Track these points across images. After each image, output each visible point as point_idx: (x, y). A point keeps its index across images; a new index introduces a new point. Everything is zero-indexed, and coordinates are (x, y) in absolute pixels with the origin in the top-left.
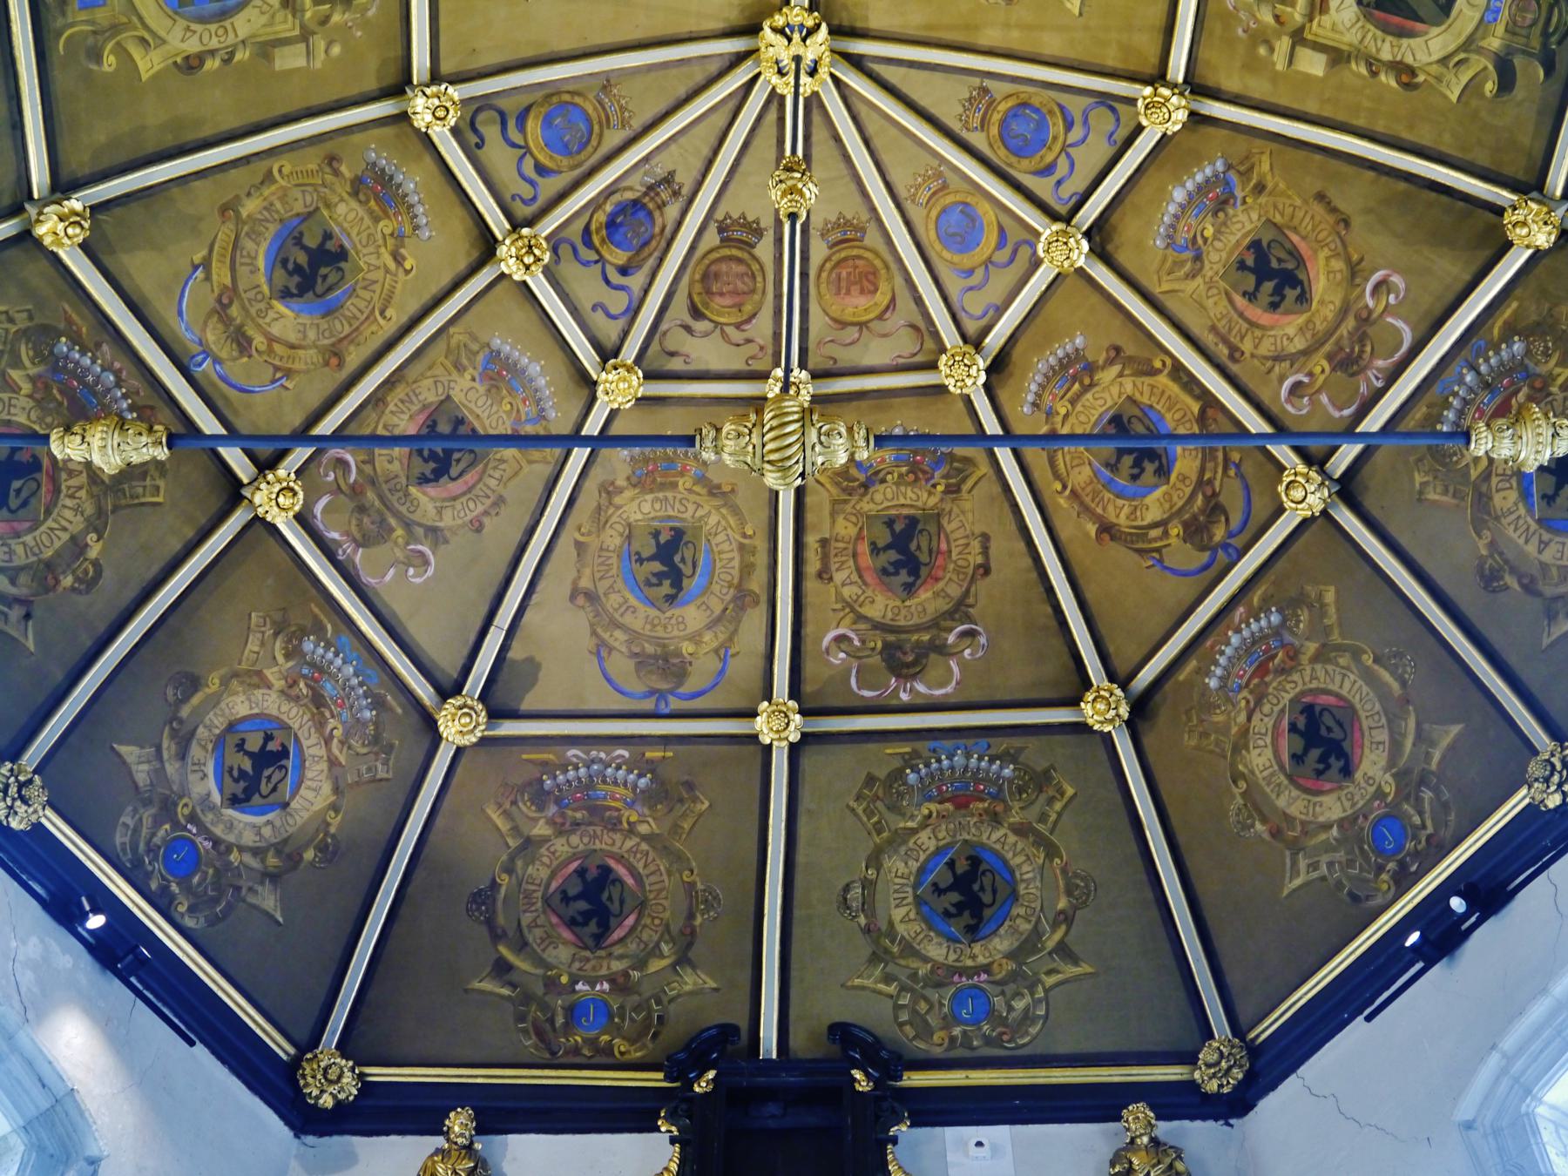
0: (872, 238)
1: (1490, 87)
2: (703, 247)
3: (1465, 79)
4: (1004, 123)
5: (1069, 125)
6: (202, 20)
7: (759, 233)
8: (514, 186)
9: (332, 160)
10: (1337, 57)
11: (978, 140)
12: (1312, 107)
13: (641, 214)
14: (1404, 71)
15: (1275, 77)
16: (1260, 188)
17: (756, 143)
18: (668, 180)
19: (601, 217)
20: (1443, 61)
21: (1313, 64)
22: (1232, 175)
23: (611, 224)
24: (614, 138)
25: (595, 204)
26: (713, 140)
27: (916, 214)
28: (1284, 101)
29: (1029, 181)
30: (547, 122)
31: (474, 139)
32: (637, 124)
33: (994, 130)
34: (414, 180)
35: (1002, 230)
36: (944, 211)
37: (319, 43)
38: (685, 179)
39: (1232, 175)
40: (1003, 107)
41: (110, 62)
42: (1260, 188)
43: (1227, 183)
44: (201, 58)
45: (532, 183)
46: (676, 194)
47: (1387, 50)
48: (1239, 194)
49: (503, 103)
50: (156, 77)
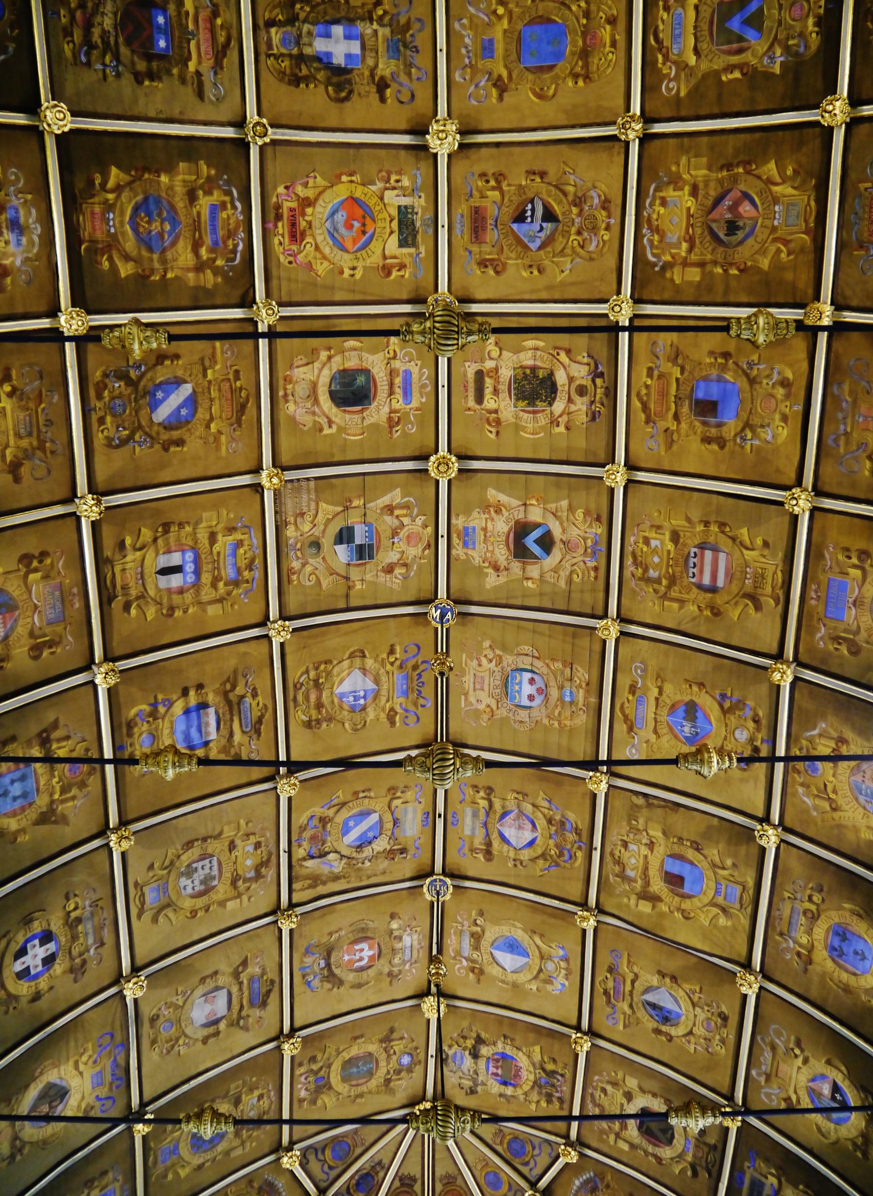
0: (459, 1181)
1: (689, 1173)
2: (394, 1187)
3: (680, 1167)
4: (509, 1143)
5: (534, 1148)
6: (205, 1151)
7: (415, 1181)
8: (320, 1175)
9: (250, 1182)
10: (633, 1146)
11: (499, 1148)
12: (625, 1160)
13: (370, 1179)
14: (659, 1160)
15: (610, 1147)
16: (608, 1186)
17: (414, 1145)
18: (380, 1163)
19: (354, 1182)
20: (672, 1159)
21: (625, 1147)
22: (597, 1180)
23: (358, 1184)
24: (358, 1151)
25: (352, 1177)
26: (397, 1145)
27: (477, 1174)
28: (615, 1155)
29: (520, 1167)
30: (333, 1150)
31: (304, 1161)
32: (367, 1144)
33: (505, 1146)
34: (281, 1183)
35: (510, 1185)
36: (487, 1173)
37: (248, 1144)
38: (386, 1162)
39: (597, 1180)
40: (508, 1137)
41: (170, 1176)
42: (608, 1186)
43: (595, 1182)
44: (203, 1164)
45: (327, 1174)
46: (383, 1168)
47: (650, 1149)
48: (600, 1186)
49: (316, 1146)
50: (187, 1176)
